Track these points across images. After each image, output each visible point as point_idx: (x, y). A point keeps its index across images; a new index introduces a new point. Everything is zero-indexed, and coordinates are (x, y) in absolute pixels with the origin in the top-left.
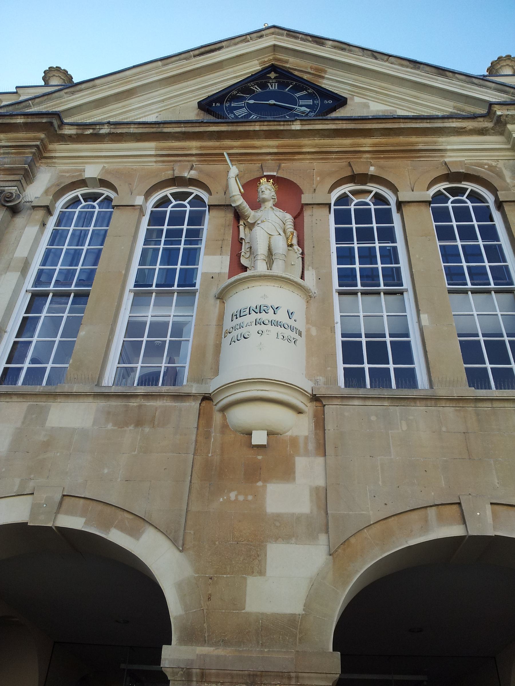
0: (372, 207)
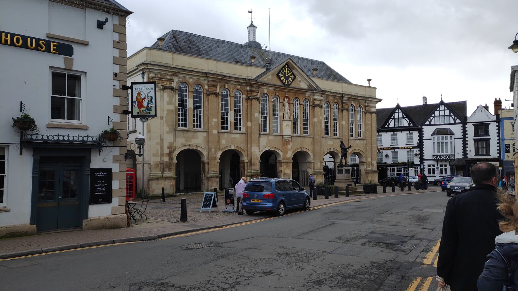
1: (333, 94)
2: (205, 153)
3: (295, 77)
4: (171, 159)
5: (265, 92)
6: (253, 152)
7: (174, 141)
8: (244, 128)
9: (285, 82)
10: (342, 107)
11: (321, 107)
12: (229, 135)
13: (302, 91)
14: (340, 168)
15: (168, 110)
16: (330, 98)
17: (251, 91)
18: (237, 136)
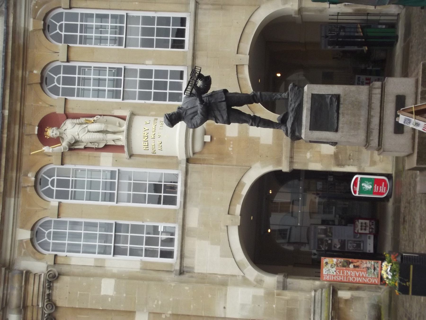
0: (62, 75)
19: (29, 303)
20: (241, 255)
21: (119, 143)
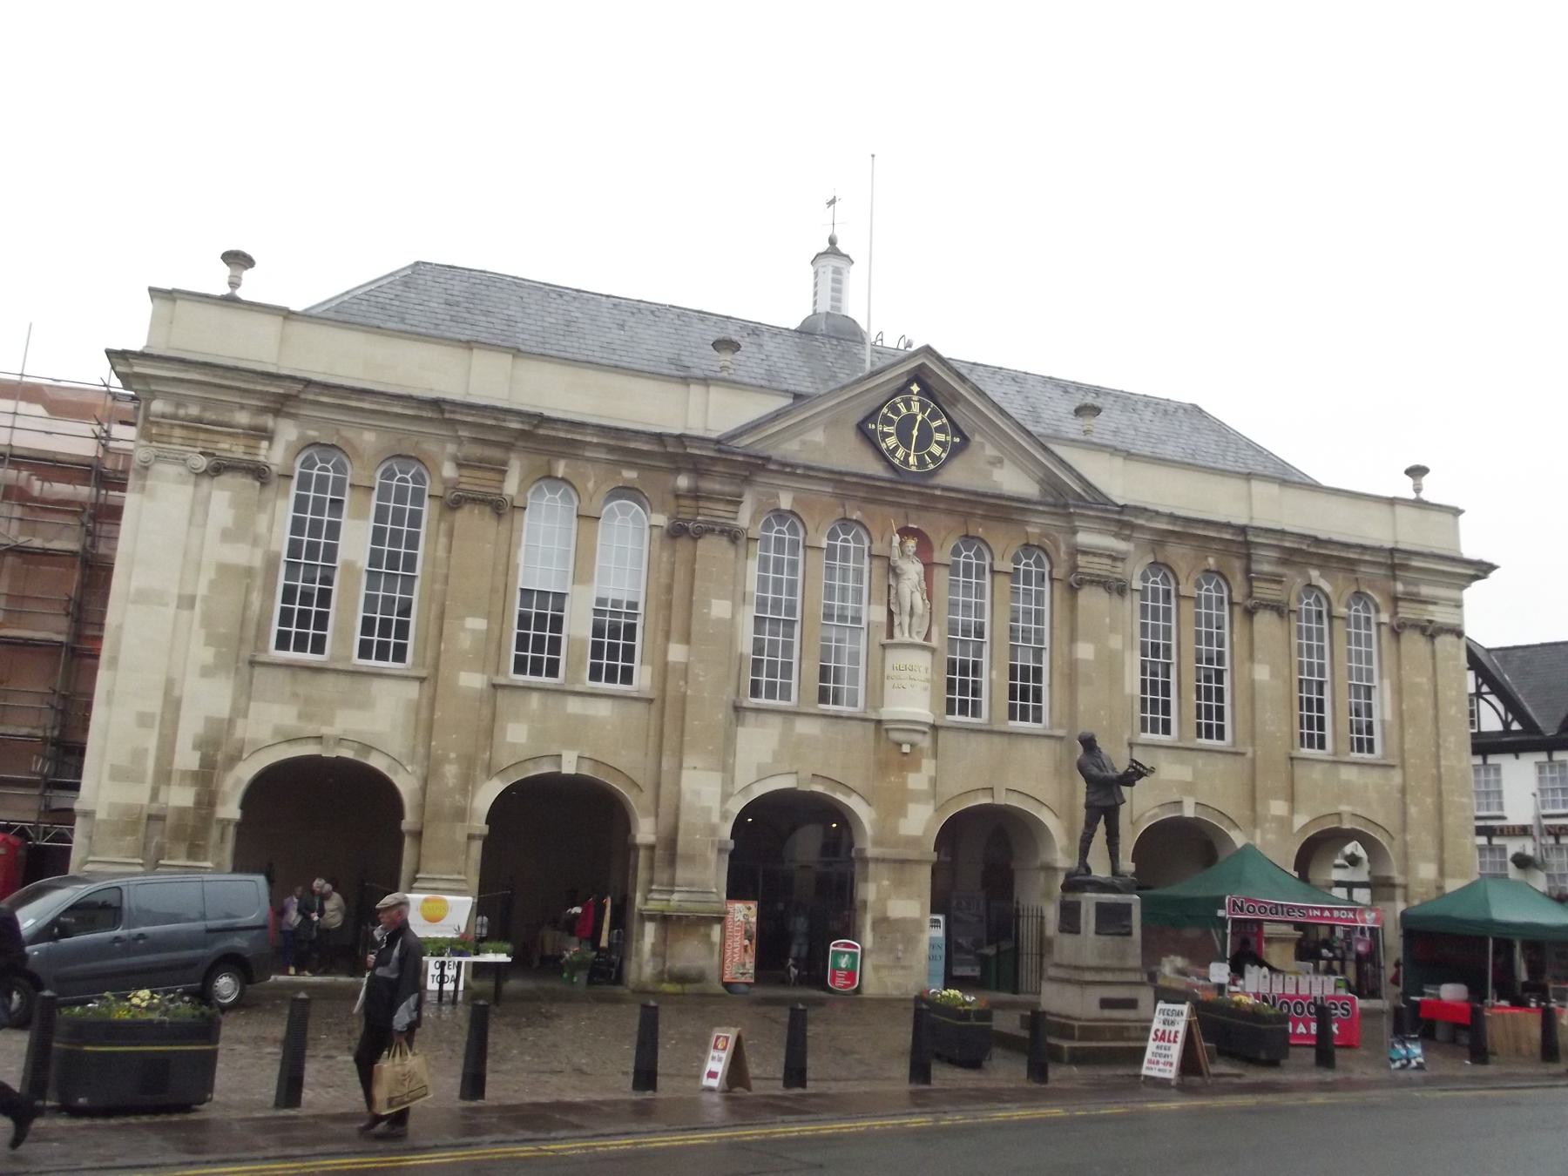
1: (1190, 531)
2: (406, 784)
3: (965, 440)
4: (208, 799)
5: (785, 502)
6: (687, 796)
7: (239, 711)
8: (648, 670)
9: (906, 461)
10: (1250, 595)
11: (1119, 589)
12: (551, 700)
13: (1003, 510)
14: (1070, 897)
15: (224, 569)
16: (1178, 554)
17: (695, 495)
18: (602, 709)
19: (701, 504)
20: (758, 791)
21: (897, 631)
